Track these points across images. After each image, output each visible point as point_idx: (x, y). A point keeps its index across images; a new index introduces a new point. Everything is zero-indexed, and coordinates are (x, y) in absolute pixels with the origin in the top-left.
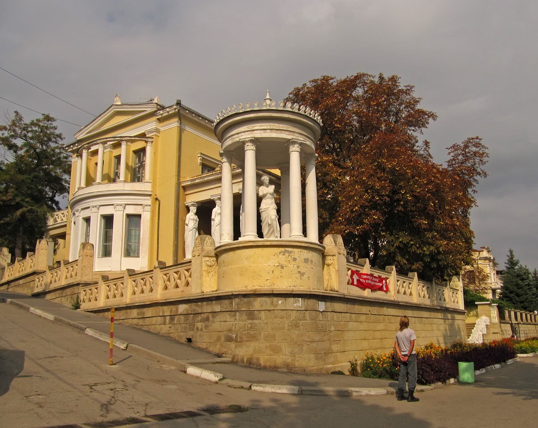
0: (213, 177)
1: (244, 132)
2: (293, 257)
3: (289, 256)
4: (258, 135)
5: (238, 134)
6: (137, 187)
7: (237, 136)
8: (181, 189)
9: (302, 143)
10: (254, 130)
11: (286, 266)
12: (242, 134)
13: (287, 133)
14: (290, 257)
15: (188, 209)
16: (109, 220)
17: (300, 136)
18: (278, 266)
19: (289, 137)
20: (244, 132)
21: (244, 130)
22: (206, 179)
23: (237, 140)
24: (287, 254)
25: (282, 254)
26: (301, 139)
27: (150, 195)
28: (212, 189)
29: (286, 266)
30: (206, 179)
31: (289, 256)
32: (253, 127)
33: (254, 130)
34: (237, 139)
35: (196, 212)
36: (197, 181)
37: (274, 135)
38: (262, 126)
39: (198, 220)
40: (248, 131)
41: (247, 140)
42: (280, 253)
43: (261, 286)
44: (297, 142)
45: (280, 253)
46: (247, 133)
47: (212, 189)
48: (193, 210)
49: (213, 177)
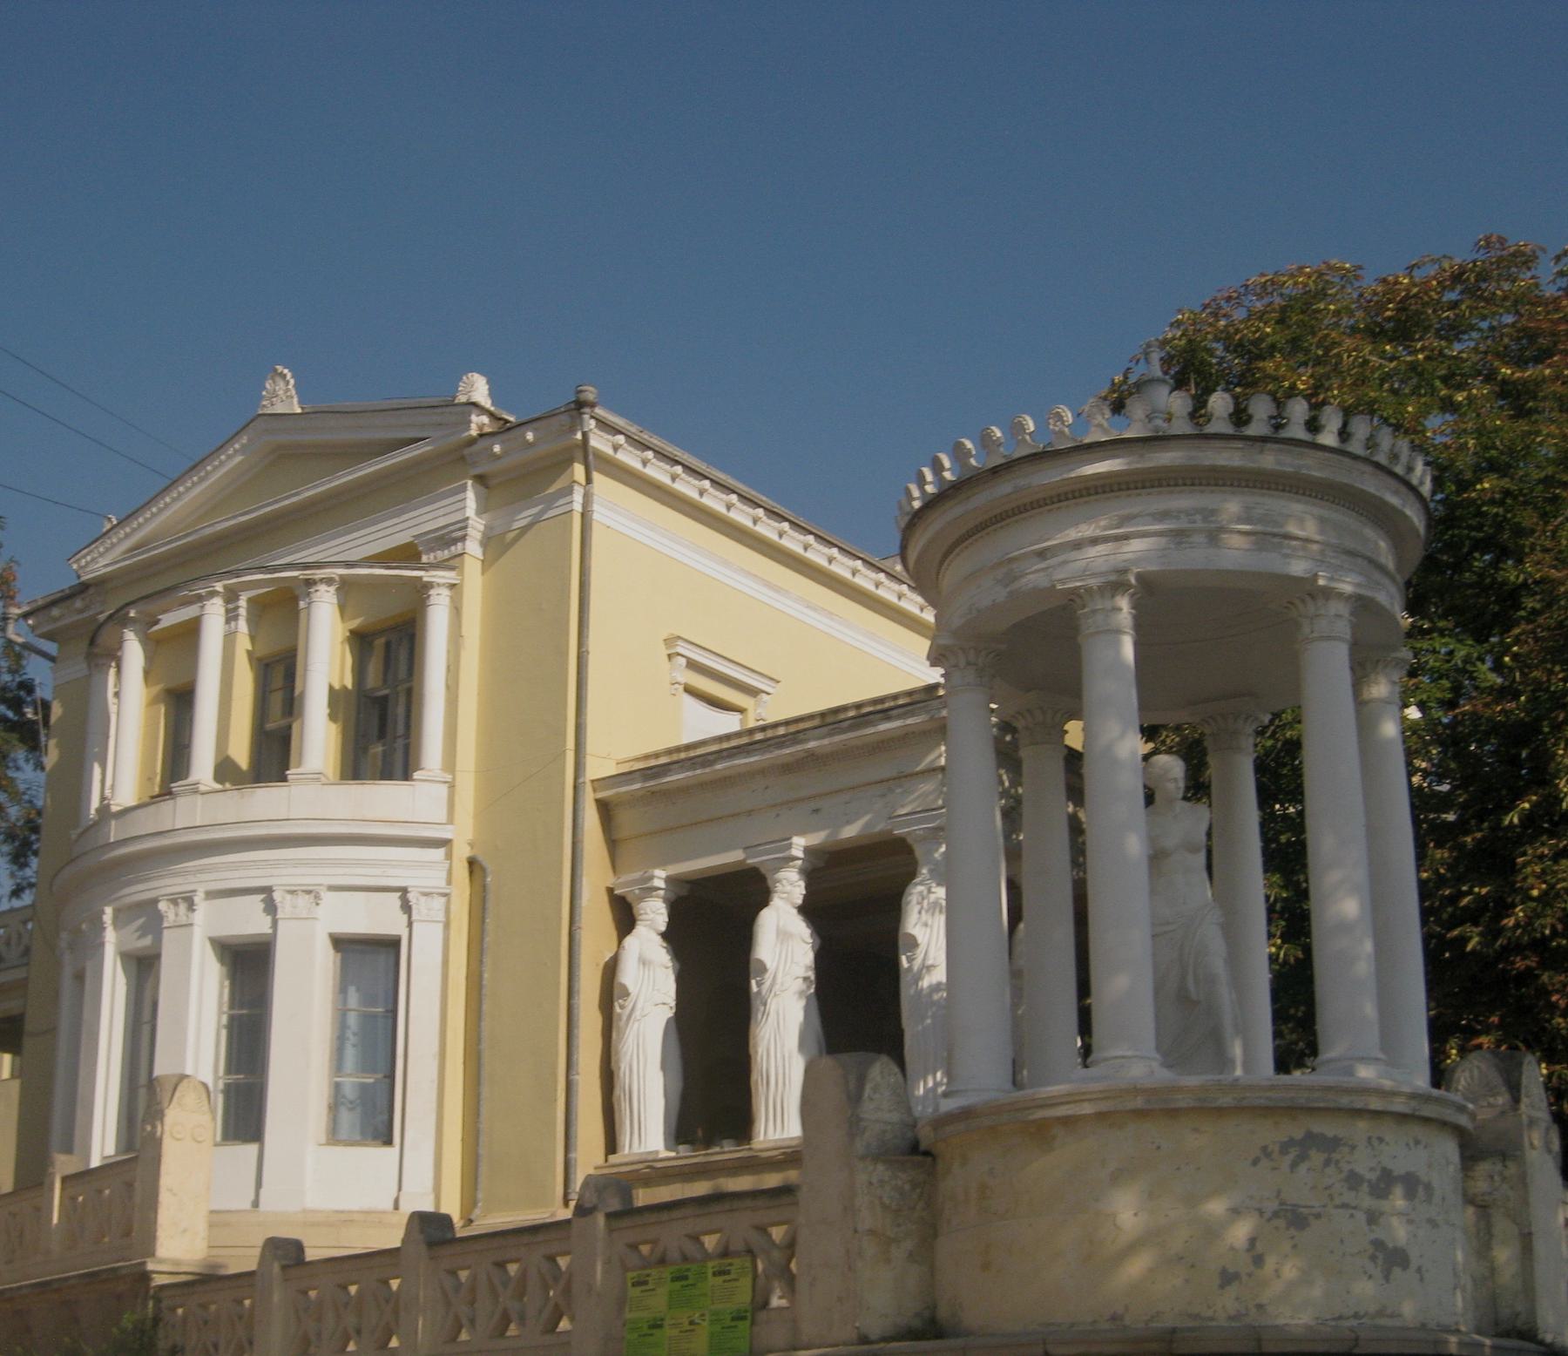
2: (1346, 1167)
3: (1327, 1163)
6: (382, 801)
11: (1318, 1216)
14: (1331, 1170)
15: (625, 917)
16: (248, 964)
18: (1276, 1214)
24: (1317, 1157)
25: (1293, 1153)
27: (444, 843)
28: (750, 813)
29: (1318, 1216)
31: (1327, 1163)
35: (669, 925)
41: (1093, 582)
42: (1285, 1148)
43: (1197, 1316)
45: (1285, 1148)
47: (750, 813)
48: (654, 914)
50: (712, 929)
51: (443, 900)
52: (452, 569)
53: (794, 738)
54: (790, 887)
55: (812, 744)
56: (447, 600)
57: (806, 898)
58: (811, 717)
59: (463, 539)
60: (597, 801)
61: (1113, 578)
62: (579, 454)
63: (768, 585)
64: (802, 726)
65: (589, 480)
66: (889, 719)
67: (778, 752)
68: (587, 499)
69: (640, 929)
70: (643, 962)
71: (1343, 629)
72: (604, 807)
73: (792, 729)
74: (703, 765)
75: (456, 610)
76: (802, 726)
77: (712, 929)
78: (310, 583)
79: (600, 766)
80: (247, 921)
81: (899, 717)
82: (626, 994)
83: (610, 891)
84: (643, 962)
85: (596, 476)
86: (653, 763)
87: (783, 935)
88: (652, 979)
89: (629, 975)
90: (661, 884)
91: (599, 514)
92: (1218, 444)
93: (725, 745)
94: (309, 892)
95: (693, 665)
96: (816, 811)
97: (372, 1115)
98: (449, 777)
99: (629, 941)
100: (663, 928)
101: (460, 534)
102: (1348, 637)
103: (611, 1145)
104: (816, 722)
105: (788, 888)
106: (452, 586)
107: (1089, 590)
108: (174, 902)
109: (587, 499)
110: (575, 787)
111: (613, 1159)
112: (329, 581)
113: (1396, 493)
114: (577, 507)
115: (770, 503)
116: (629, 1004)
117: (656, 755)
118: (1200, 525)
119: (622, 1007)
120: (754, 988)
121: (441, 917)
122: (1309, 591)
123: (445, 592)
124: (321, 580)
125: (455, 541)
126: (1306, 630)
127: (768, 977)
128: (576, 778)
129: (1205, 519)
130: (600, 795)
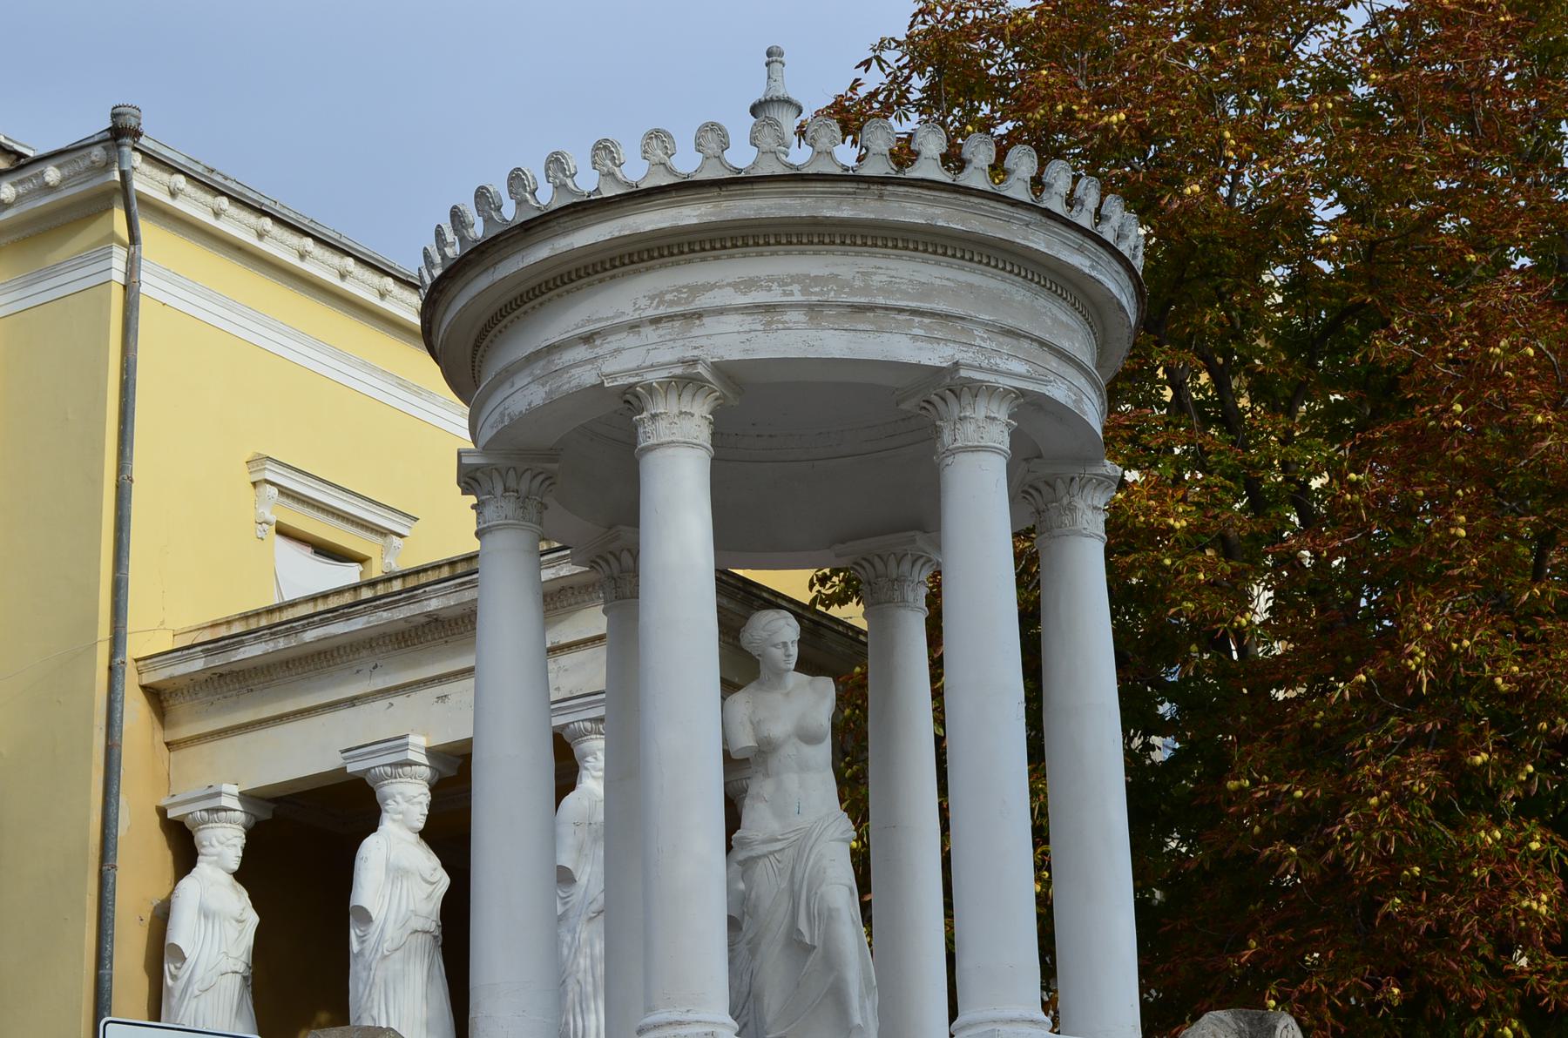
0: (357, 624)
1: (634, 327)
4: (729, 340)
5: (588, 339)
7: (581, 352)
8: (135, 708)
9: (1022, 393)
10: (698, 315)
12: (618, 337)
13: (918, 327)
15: (184, 847)
17: (1007, 345)
19: (934, 355)
20: (634, 327)
21: (631, 315)
22: (310, 636)
23: (587, 377)
26: (1014, 367)
28: (352, 702)
30: (310, 636)
32: (696, 290)
33: (698, 315)
34: (584, 371)
36: (251, 651)
37: (834, 343)
38: (749, 284)
39: (253, 919)
40: (656, 321)
44: (992, 391)
46: (650, 334)
47: (352, 702)
49: (357, 624)
53: (410, 595)
55: (434, 605)
57: (431, 818)
58: (437, 567)
60: (145, 688)
61: (678, 371)
62: (119, 199)
63: (402, 384)
64: (423, 579)
65: (134, 239)
67: (385, 615)
68: (132, 265)
69: (203, 868)
70: (206, 914)
71: (999, 436)
72: (157, 696)
73: (412, 582)
74: (287, 634)
76: (423, 579)
82: (180, 956)
83: (162, 812)
84: (206, 914)
86: (223, 632)
89: (182, 933)
90: (235, 804)
91: (150, 285)
92: (819, 187)
93: (321, 607)
96: (442, 698)
99: (186, 882)
100: (236, 867)
102: (1006, 446)
104: (445, 572)
105: (404, 806)
107: (650, 389)
109: (132, 265)
113: (1080, 250)
114: (118, 276)
116: (184, 974)
117: (228, 622)
118: (798, 297)
119: (174, 978)
120: (355, 946)
122: (947, 386)
126: (947, 437)
127: (374, 930)
128: (112, 656)
129: (804, 291)
130: (150, 678)
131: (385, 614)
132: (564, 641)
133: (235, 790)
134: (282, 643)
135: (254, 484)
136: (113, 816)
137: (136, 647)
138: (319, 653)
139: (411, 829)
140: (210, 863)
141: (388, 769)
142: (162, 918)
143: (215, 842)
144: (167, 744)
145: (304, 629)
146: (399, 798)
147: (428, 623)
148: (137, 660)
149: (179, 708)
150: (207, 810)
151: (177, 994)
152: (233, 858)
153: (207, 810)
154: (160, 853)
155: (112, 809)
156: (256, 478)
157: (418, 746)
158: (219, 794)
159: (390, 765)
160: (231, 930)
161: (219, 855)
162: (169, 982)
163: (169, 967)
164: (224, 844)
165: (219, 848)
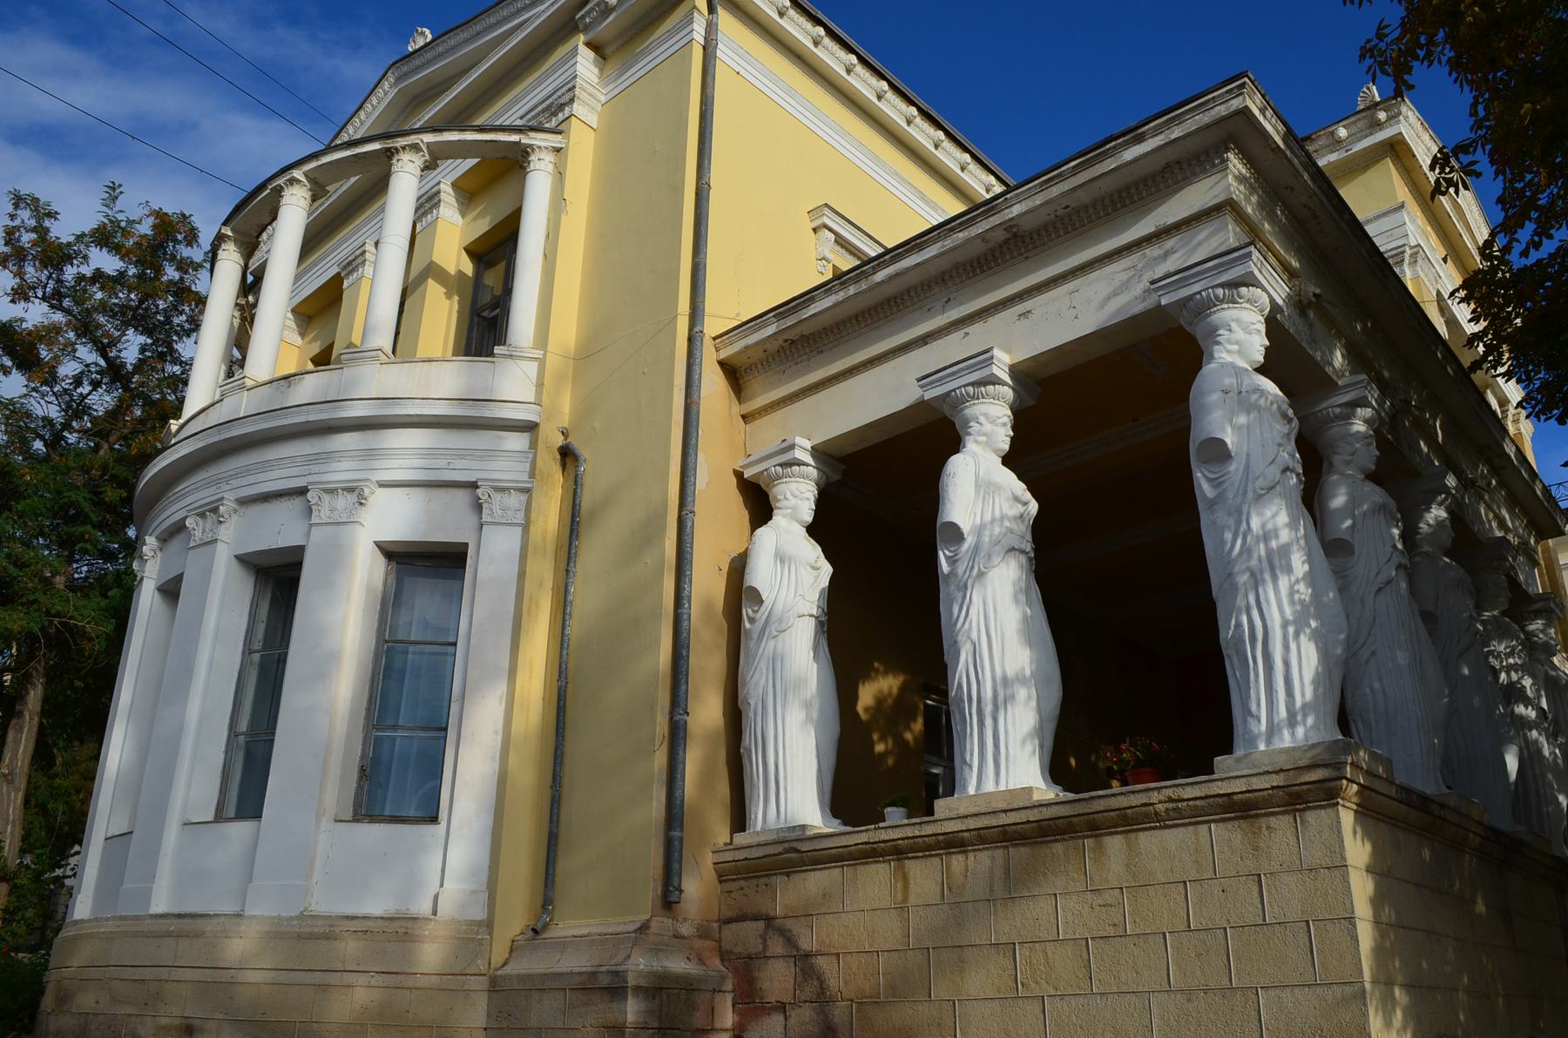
15: (759, 504)
30: (880, 276)
39: (827, 570)
50: (880, 511)
51: (524, 497)
52: (560, 133)
54: (991, 422)
55: (1016, 210)
56: (550, 168)
59: (572, 100)
60: (721, 363)
63: (923, 197)
66: (1140, 139)
68: (711, 29)
69: (778, 518)
70: (781, 558)
72: (734, 373)
75: (560, 175)
77: (880, 511)
78: (389, 154)
79: (723, 312)
80: (276, 530)
81: (1157, 132)
83: (738, 475)
84: (781, 558)
85: (720, 10)
87: (985, 488)
88: (793, 573)
89: (761, 575)
90: (808, 459)
94: (351, 490)
95: (841, 241)
97: (397, 775)
98: (538, 354)
100: (809, 518)
101: (567, 98)
103: (739, 820)
105: (988, 427)
106: (558, 150)
108: (202, 515)
109: (711, 29)
110: (690, 340)
111: (740, 839)
112: (415, 148)
115: (925, 106)
116: (762, 615)
119: (752, 620)
120: (944, 566)
121: (520, 518)
123: (549, 158)
124: (403, 148)
125: (561, 107)
128: (691, 329)
130: (723, 354)
131: (961, 235)
132: (1171, 220)
133: (808, 445)
134: (852, 290)
135: (815, 230)
136: (691, 465)
137: (713, 325)
138: (888, 300)
139: (996, 451)
140: (784, 516)
141: (970, 389)
142: (739, 567)
143: (789, 496)
144: (743, 417)
145: (875, 271)
146: (982, 419)
147: (1007, 241)
148: (714, 339)
149: (753, 383)
150: (780, 465)
151: (755, 636)
152: (807, 512)
153: (780, 465)
154: (738, 512)
155: (691, 459)
156: (815, 224)
157: (1002, 361)
158: (792, 447)
159: (972, 384)
160: (807, 576)
161: (794, 508)
162: (748, 625)
163: (747, 611)
164: (798, 498)
165: (793, 501)
